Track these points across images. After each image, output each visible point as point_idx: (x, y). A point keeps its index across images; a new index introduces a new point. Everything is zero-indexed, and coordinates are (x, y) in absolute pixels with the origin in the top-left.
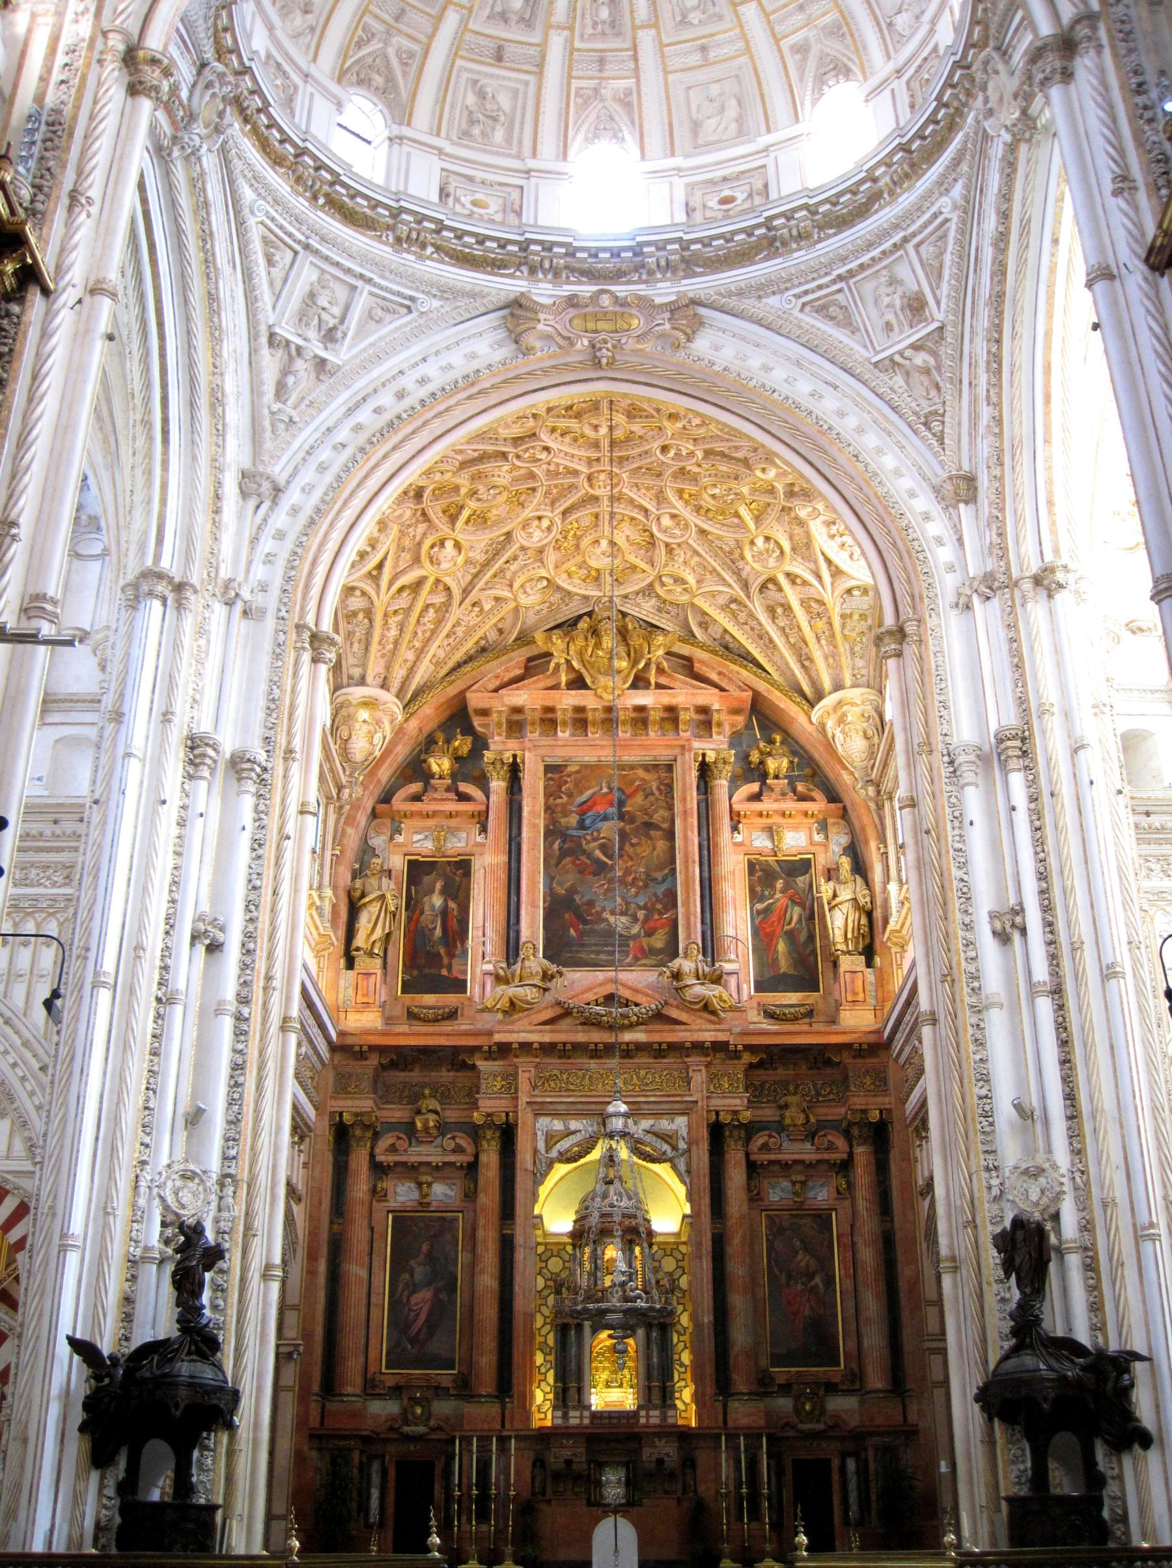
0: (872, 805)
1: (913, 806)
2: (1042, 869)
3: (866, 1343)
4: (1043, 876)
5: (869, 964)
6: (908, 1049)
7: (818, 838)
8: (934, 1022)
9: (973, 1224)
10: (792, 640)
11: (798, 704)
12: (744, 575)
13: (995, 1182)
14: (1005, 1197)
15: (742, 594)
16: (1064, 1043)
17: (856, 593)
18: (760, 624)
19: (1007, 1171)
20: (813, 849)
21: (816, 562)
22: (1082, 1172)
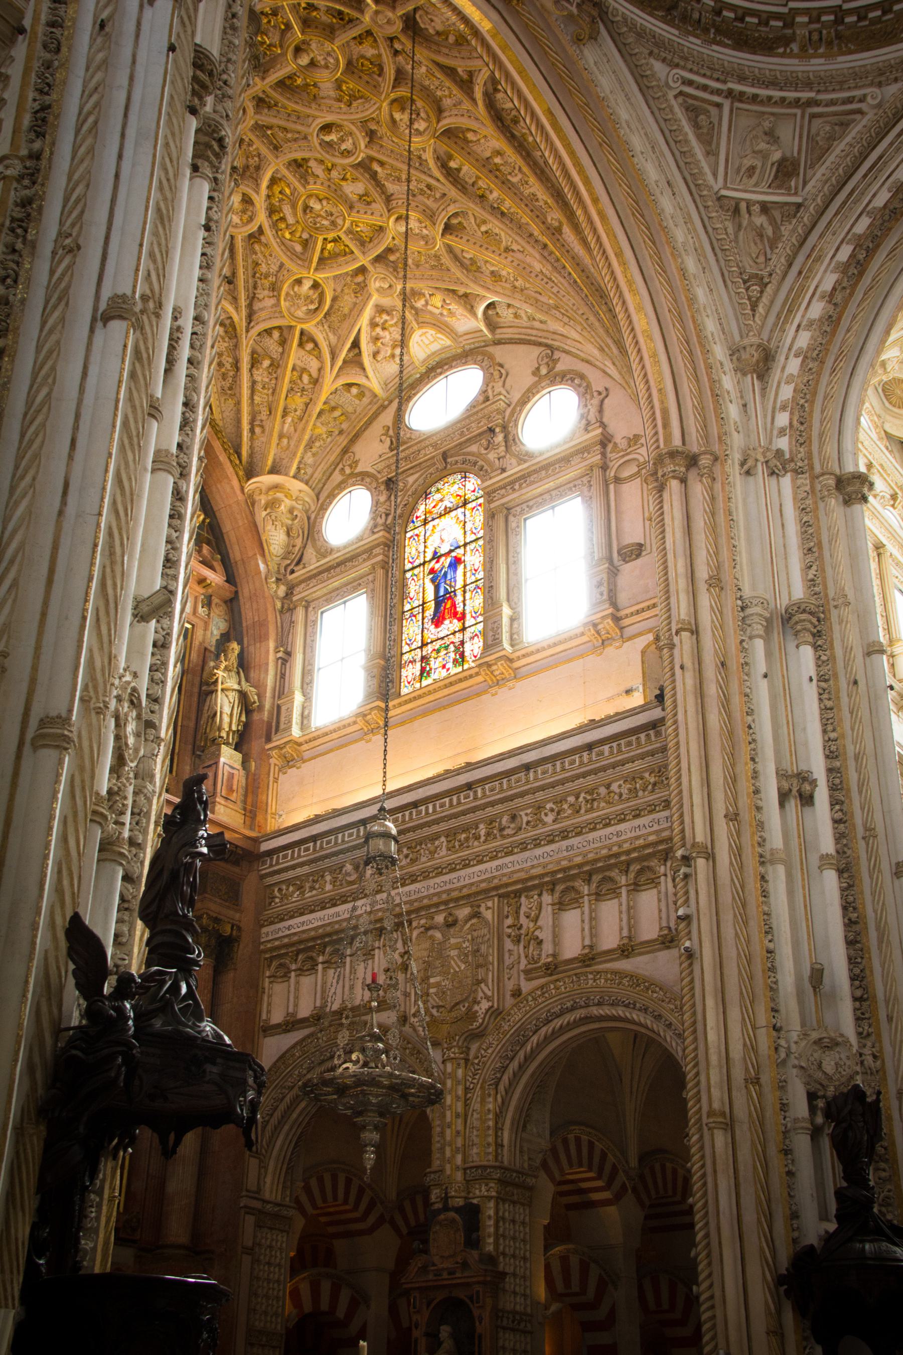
0: (279, 605)
1: (692, 633)
2: (833, 748)
3: (172, 1187)
4: (830, 755)
5: (245, 763)
6: (299, 871)
7: (201, 611)
8: (710, 856)
9: (756, 1081)
10: (257, 399)
11: (234, 466)
12: (255, 308)
13: (782, 1042)
14: (793, 1061)
15: (244, 324)
16: (849, 924)
17: (354, 390)
18: (236, 366)
19: (794, 1036)
20: (195, 620)
21: (341, 340)
22: (875, 1057)
